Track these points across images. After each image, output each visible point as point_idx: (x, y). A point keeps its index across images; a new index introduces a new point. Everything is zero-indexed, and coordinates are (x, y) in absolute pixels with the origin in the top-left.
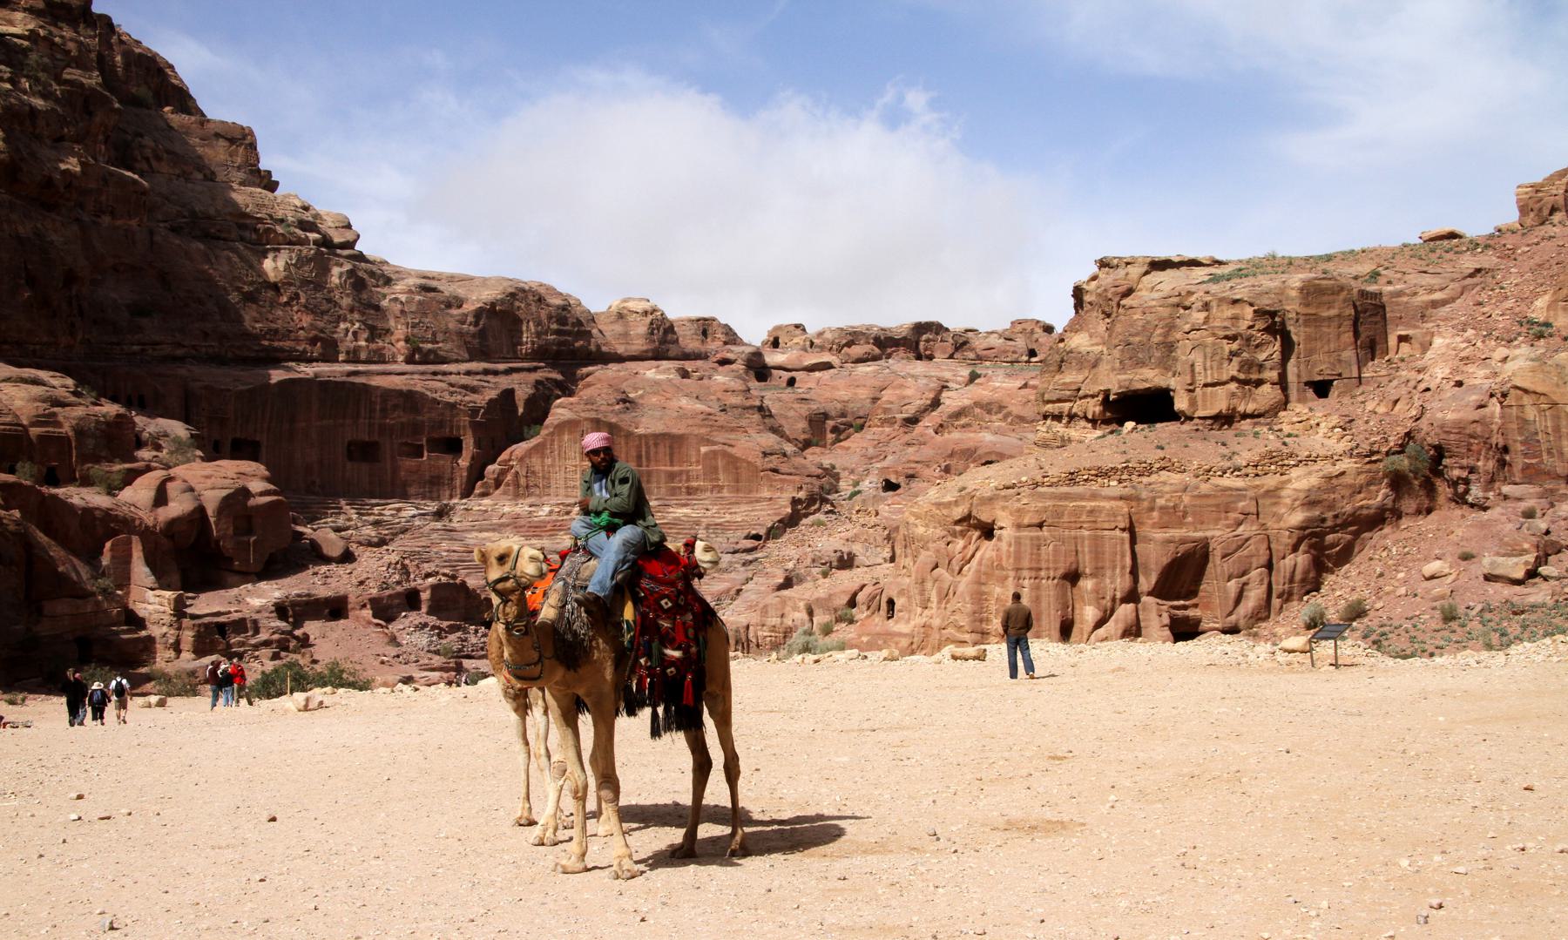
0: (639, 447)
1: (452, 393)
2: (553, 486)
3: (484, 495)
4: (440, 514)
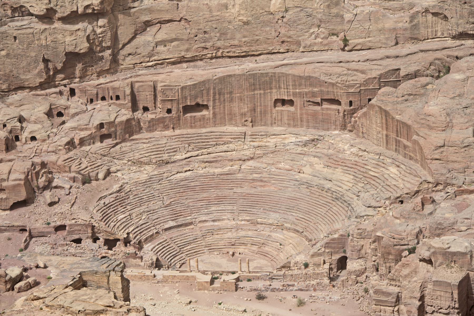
0: (397, 126)
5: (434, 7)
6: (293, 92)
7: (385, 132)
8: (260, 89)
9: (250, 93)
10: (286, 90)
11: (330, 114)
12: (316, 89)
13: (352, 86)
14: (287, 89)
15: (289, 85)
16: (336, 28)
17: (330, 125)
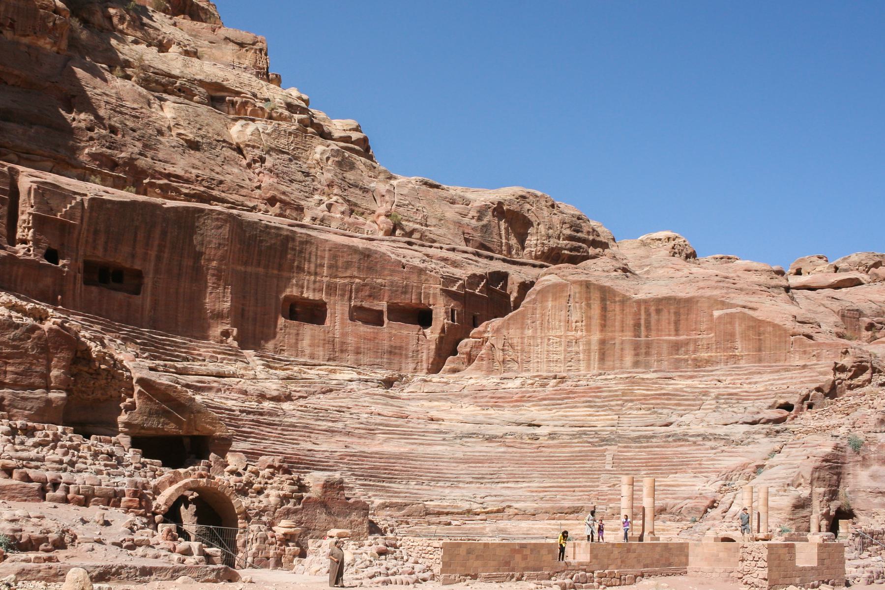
0: (638, 313)
1: (424, 261)
2: (534, 359)
3: (455, 371)
4: (388, 383)
5: (511, 202)
7: (596, 337)
8: (259, 265)
11: (407, 336)
13: (452, 280)
15: (322, 266)
16: (359, 202)
17: (404, 361)
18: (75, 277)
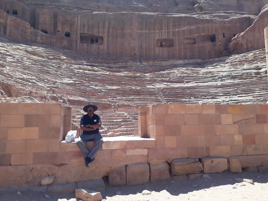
6: (173, 32)
8: (146, 29)
9: (139, 31)
10: (167, 31)
12: (192, 27)
14: (168, 29)
15: (170, 26)
18: (77, 41)
